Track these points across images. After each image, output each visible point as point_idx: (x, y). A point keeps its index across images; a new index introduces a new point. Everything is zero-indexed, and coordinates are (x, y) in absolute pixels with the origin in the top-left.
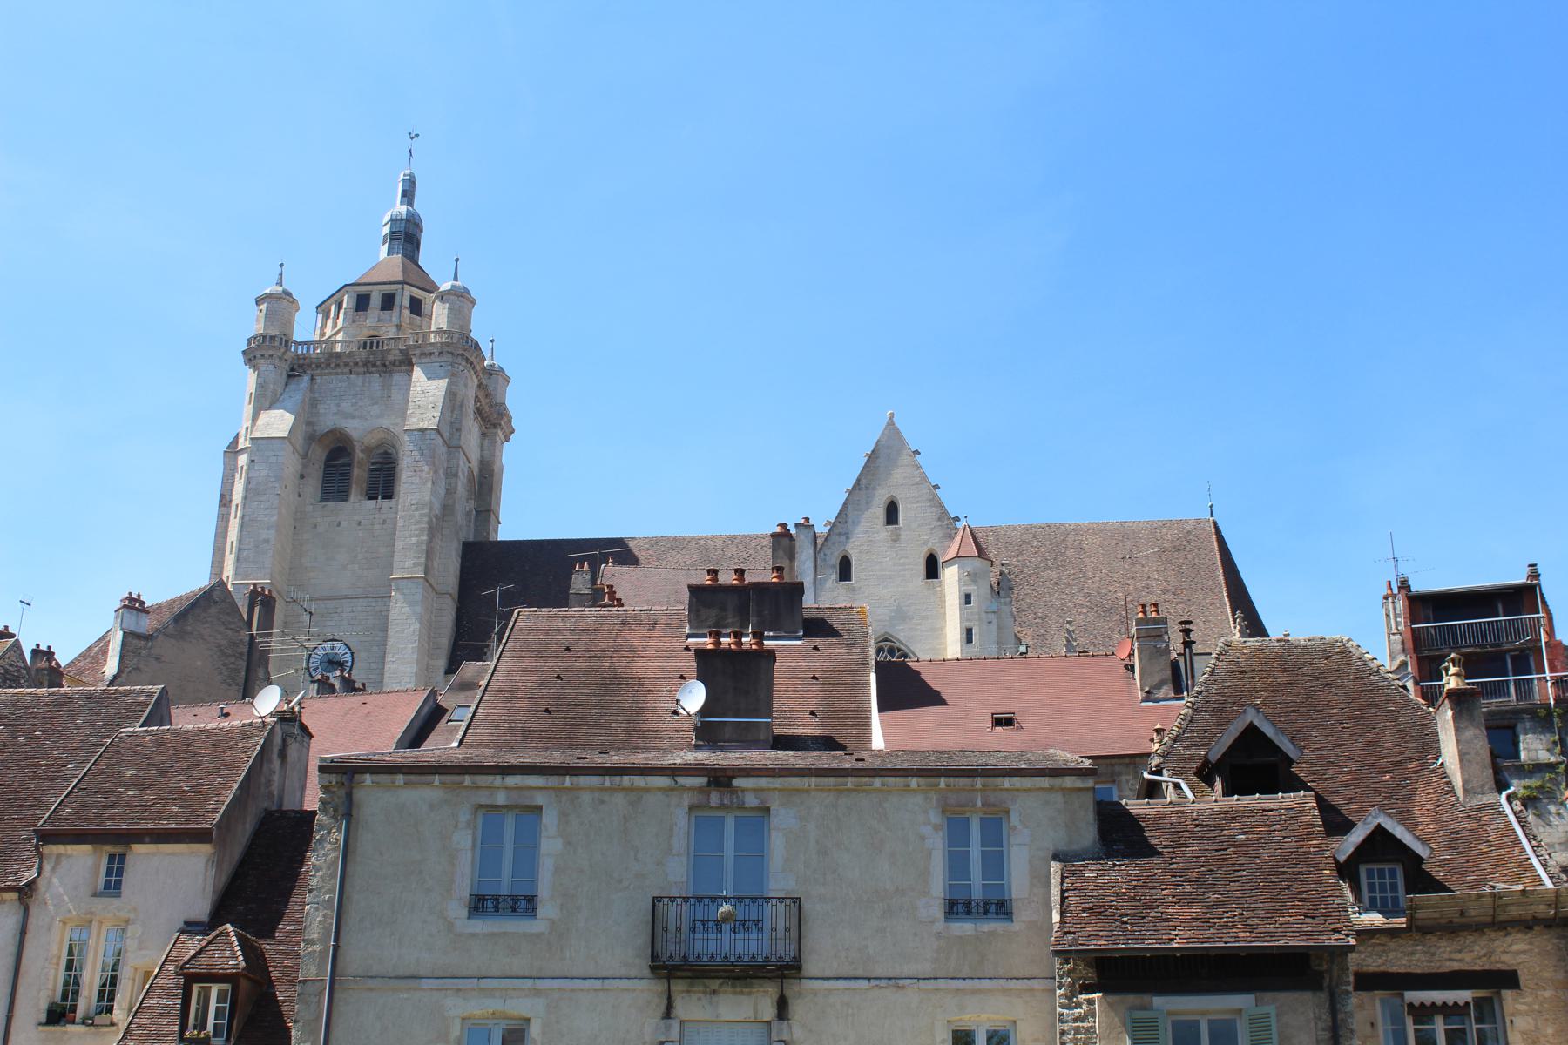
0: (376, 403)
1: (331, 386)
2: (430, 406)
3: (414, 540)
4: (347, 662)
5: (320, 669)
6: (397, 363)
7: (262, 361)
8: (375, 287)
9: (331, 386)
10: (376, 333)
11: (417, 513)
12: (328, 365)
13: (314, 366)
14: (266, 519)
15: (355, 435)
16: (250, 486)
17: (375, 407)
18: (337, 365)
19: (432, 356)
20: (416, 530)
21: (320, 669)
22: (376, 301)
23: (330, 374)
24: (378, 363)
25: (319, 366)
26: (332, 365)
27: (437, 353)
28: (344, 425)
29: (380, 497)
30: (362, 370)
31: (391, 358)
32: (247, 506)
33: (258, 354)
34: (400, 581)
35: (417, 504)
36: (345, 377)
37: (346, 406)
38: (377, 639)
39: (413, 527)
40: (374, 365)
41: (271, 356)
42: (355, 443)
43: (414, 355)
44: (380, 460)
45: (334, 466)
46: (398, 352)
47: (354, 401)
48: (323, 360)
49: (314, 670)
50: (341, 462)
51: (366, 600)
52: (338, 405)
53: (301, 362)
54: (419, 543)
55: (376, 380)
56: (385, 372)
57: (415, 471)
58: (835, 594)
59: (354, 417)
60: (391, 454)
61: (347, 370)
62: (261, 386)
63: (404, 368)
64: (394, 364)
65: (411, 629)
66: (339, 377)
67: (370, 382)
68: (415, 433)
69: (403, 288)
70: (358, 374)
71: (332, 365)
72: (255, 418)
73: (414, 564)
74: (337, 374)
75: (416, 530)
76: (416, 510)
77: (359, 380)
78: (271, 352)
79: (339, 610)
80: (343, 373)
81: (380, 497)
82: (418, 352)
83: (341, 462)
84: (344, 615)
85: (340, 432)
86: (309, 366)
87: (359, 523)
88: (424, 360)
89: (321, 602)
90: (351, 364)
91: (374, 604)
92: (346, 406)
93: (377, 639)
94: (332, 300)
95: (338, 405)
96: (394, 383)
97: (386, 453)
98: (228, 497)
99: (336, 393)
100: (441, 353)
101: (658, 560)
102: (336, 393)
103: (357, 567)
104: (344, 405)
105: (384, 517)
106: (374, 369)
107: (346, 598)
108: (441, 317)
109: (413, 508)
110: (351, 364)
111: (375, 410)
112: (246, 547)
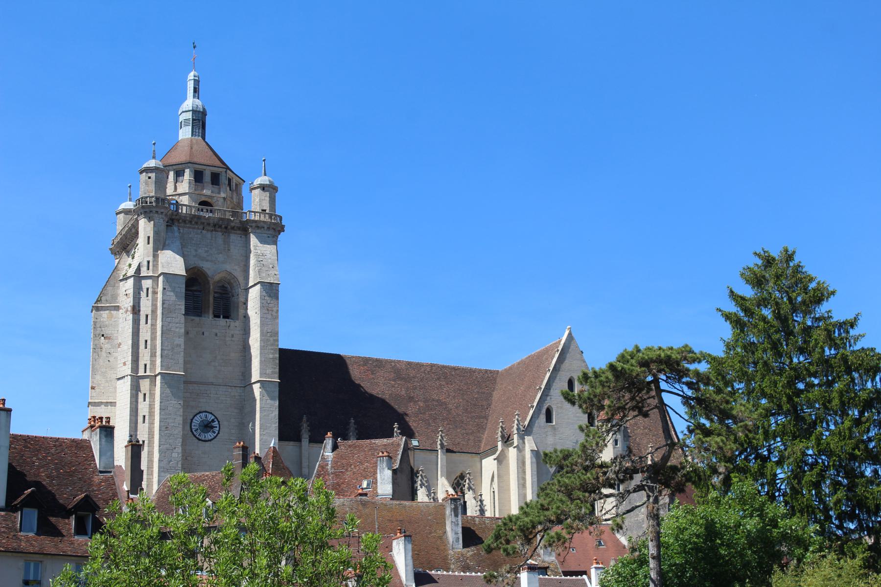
0: (221, 253)
1: (190, 236)
2: (271, 266)
3: (271, 356)
4: (216, 427)
5: (199, 431)
6: (236, 228)
7: (156, 215)
8: (208, 168)
9: (190, 236)
10: (209, 200)
11: (271, 339)
12: (191, 222)
13: (180, 221)
14: (177, 330)
15: (209, 273)
16: (165, 306)
17: (221, 255)
18: (196, 223)
19: (263, 229)
20: (272, 349)
21: (199, 431)
22: (207, 177)
23: (189, 228)
24: (223, 226)
25: (185, 221)
26: (193, 223)
27: (266, 228)
28: (201, 265)
29: (222, 316)
30: (211, 228)
31: (233, 224)
32: (164, 320)
33: (154, 210)
34: (264, 382)
35: (271, 332)
36: (200, 231)
37: (201, 251)
38: (233, 414)
39: (270, 347)
40: (220, 227)
41: (162, 213)
42: (209, 279)
43: (252, 226)
44: (219, 291)
45: (191, 291)
46: (238, 221)
47: (206, 249)
48: (188, 219)
49: (195, 431)
50: (195, 288)
51: (225, 387)
52: (196, 251)
53: (174, 217)
54: (274, 359)
55: (219, 237)
56: (225, 232)
57: (268, 310)
58: (546, 430)
59: (207, 261)
60: (226, 288)
61: (201, 227)
62: (156, 233)
63: (239, 232)
64: (233, 228)
65: (273, 414)
66: (195, 230)
67: (216, 238)
68: (266, 284)
69: (226, 172)
70: (208, 230)
71: (193, 223)
72: (155, 256)
73: (272, 372)
74: (194, 228)
75: (272, 349)
76: (271, 336)
77: (209, 235)
78: (162, 211)
79: (208, 392)
80: (198, 228)
81: (222, 316)
82: (254, 225)
83: (195, 288)
84: (212, 396)
85: (198, 270)
86: (178, 221)
87: (216, 335)
88: (257, 231)
89: (196, 385)
90: (206, 224)
91: (230, 390)
92: (201, 251)
93: (233, 414)
94: (174, 167)
95: (196, 251)
96: (231, 241)
97: (223, 286)
98: (137, 307)
99: (194, 242)
100: (268, 228)
101: (372, 374)
102: (194, 242)
103: (217, 364)
104: (200, 251)
105: (232, 332)
106: (220, 229)
107: (212, 384)
108: (264, 201)
109: (269, 335)
110: (206, 224)
111: (221, 257)
112: (167, 348)
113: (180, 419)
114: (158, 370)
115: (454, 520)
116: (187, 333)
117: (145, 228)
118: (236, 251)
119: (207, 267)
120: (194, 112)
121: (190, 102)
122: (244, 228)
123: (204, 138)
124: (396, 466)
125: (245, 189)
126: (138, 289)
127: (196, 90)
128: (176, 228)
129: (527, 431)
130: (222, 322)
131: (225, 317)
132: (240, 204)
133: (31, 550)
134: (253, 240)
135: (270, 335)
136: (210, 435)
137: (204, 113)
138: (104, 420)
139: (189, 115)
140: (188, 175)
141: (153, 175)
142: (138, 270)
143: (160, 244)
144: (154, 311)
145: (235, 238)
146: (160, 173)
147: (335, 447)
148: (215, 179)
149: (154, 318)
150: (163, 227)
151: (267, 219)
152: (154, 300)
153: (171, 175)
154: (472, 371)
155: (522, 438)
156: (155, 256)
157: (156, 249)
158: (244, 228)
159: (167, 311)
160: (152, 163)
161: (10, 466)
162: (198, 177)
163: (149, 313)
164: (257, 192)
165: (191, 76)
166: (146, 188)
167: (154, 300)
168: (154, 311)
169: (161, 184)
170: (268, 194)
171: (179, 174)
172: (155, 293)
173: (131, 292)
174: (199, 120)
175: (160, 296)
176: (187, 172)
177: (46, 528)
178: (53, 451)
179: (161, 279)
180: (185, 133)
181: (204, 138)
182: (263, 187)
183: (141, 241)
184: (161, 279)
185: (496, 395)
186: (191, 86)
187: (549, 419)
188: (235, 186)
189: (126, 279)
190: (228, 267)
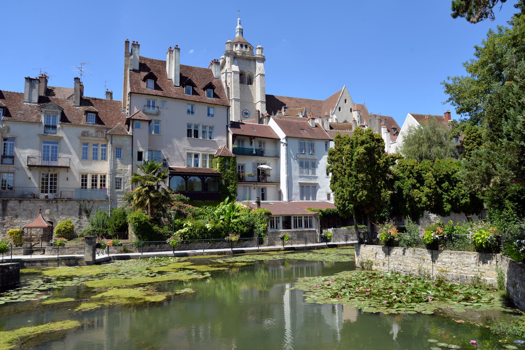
55: (248, 62)
62: (231, 61)
77: (245, 62)
113: (239, 111)
114: (233, 98)
115: (327, 122)
116: (240, 88)
117: (228, 59)
118: (252, 66)
119: (245, 71)
120: (240, 29)
121: (238, 27)
122: (255, 60)
123: (242, 36)
124: (303, 115)
125: (254, 50)
126: (226, 76)
127: (240, 23)
128: (236, 60)
129: (334, 114)
130: (250, 86)
131: (251, 84)
132: (253, 53)
133: (190, 99)
134: (257, 62)
135: (263, 89)
136: (247, 116)
137: (242, 30)
138: (216, 61)
139: (238, 30)
140: (239, 46)
141: (229, 44)
142: (226, 71)
143: (232, 63)
144: (231, 82)
145: (252, 62)
146: (232, 44)
147: (285, 111)
148: (246, 47)
149: (231, 84)
150: (233, 59)
151: (261, 57)
152: (231, 79)
153: (234, 45)
154: (316, 101)
155: (332, 115)
156: (231, 67)
157: (231, 65)
158: (255, 60)
159: (235, 82)
160: (229, 41)
161: (181, 74)
162: (242, 46)
163: (230, 82)
164: (257, 50)
165: (238, 19)
166: (228, 48)
167: (231, 79)
168: (231, 82)
169: (232, 47)
170: (260, 50)
171: (236, 45)
172: (231, 77)
173: (225, 77)
174: (241, 31)
175: (232, 77)
176: (238, 44)
177: (195, 93)
178: (198, 71)
179: (233, 73)
180: (237, 35)
181: (242, 36)
182: (259, 48)
183: (227, 64)
184: (233, 73)
185: (323, 107)
186: (238, 22)
187: (340, 110)
188: (252, 49)
189: (223, 73)
190: (250, 70)
